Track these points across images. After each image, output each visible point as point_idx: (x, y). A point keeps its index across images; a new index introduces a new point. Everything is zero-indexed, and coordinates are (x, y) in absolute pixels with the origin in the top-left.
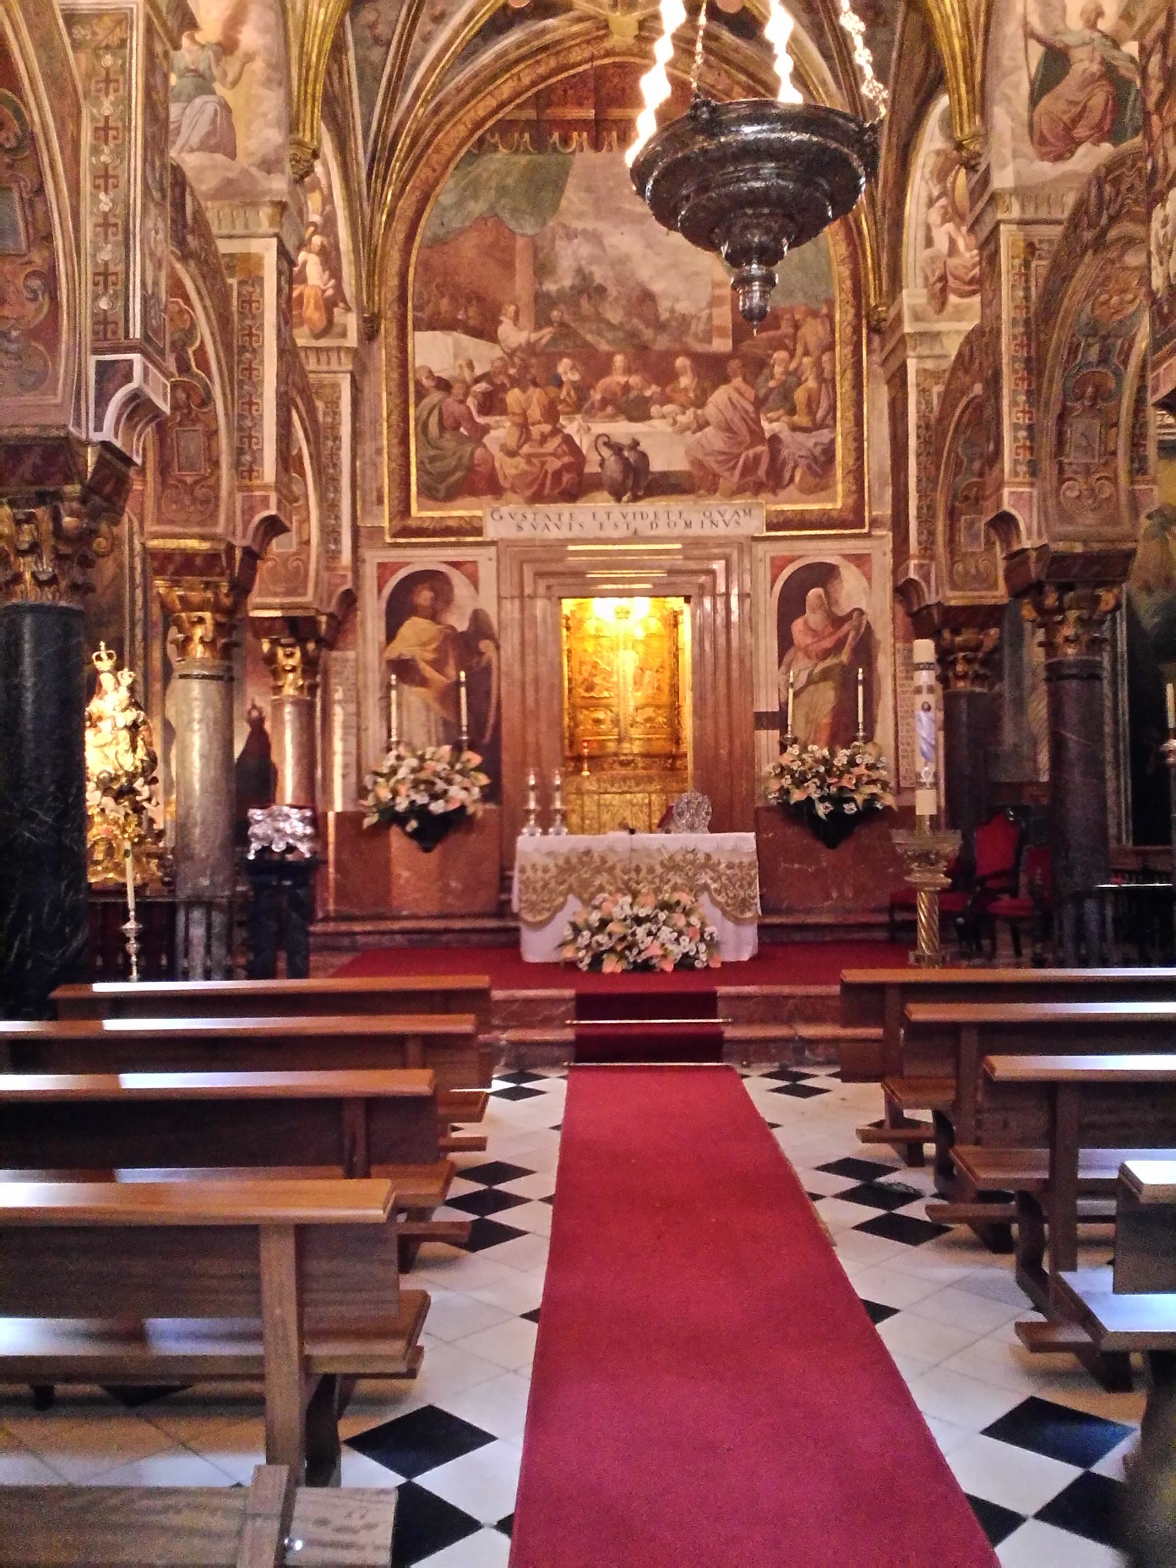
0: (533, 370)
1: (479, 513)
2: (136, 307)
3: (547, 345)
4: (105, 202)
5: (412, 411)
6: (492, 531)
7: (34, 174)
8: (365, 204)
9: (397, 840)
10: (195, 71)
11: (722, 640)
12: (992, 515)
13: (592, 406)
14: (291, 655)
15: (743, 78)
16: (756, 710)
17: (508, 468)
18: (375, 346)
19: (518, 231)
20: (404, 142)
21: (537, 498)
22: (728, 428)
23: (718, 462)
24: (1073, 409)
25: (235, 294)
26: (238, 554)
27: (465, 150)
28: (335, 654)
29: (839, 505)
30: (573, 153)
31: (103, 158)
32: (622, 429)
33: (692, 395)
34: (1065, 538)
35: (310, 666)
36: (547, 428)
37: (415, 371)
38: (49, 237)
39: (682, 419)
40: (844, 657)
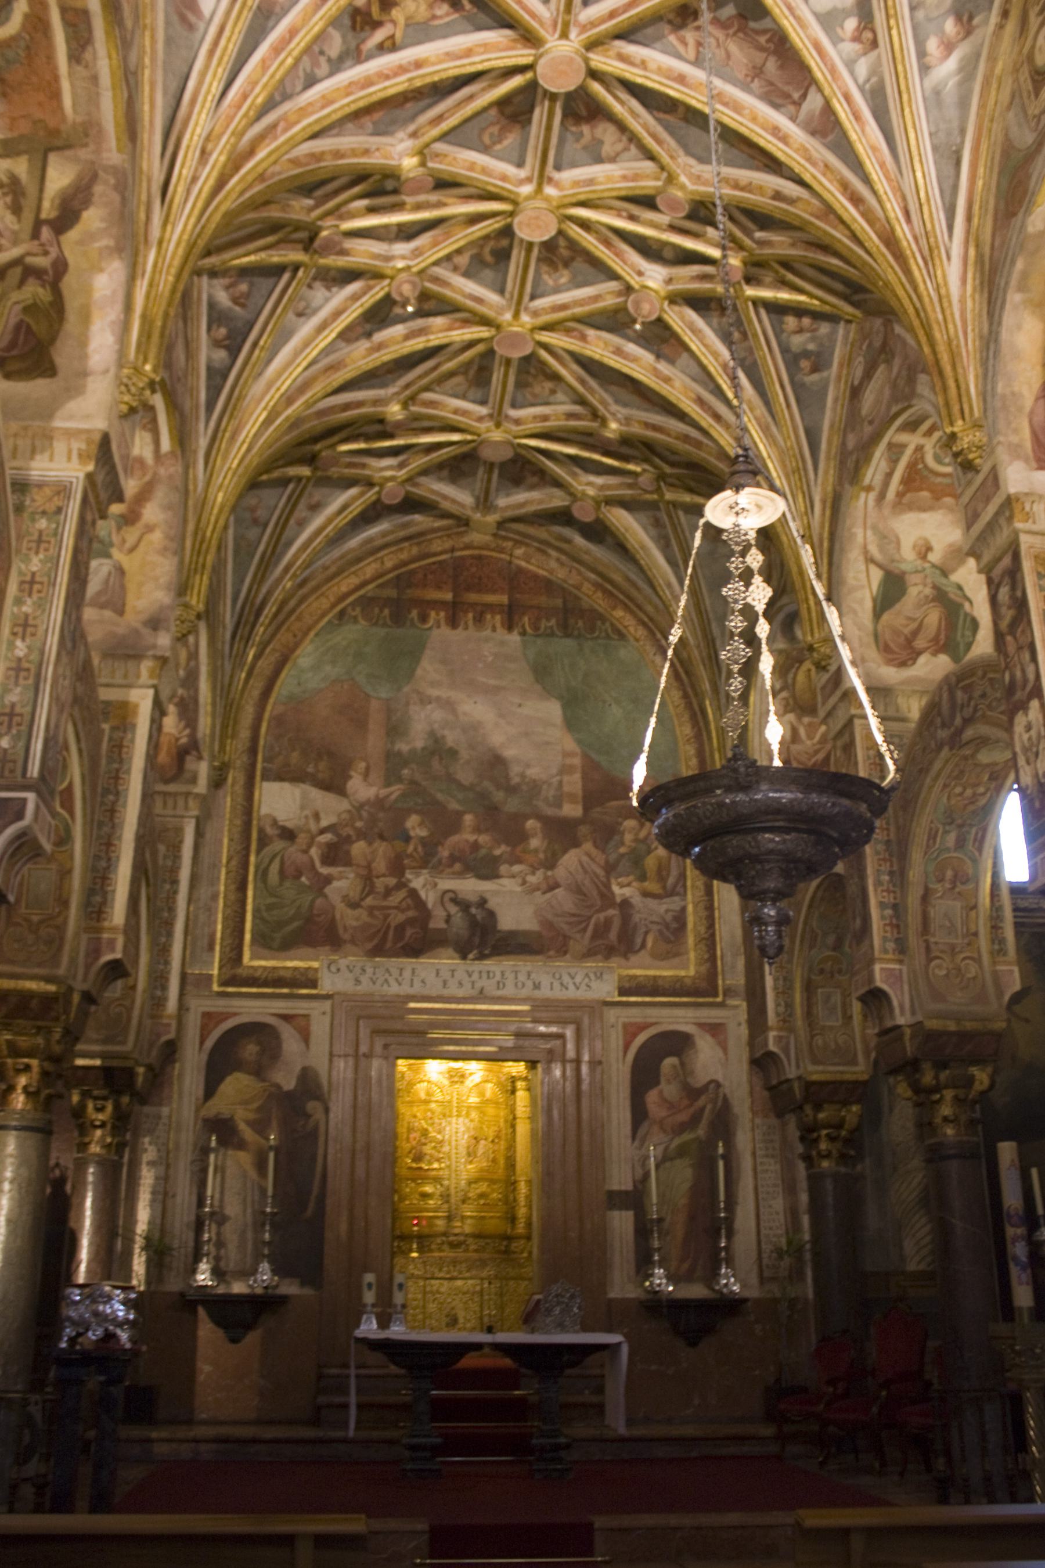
0: (381, 824)
1: (315, 964)
2: (38, 747)
3: (396, 801)
4: (21, 648)
5: (252, 859)
6: (327, 984)
8: (226, 663)
9: (206, 1330)
11: (571, 1109)
12: (862, 991)
13: (440, 862)
14: (100, 1110)
15: (593, 576)
16: (607, 1187)
17: (350, 919)
18: (221, 792)
19: (372, 693)
20: (269, 610)
21: (378, 951)
22: (578, 890)
23: (569, 924)
24: (936, 891)
25: (106, 739)
26: (76, 998)
27: (326, 619)
28: (147, 1109)
29: (692, 972)
30: (430, 629)
31: (25, 609)
32: (470, 887)
33: (541, 856)
34: (939, 1016)
35: (121, 1122)
36: (392, 881)
37: (259, 820)
39: (532, 879)
40: (701, 1132)
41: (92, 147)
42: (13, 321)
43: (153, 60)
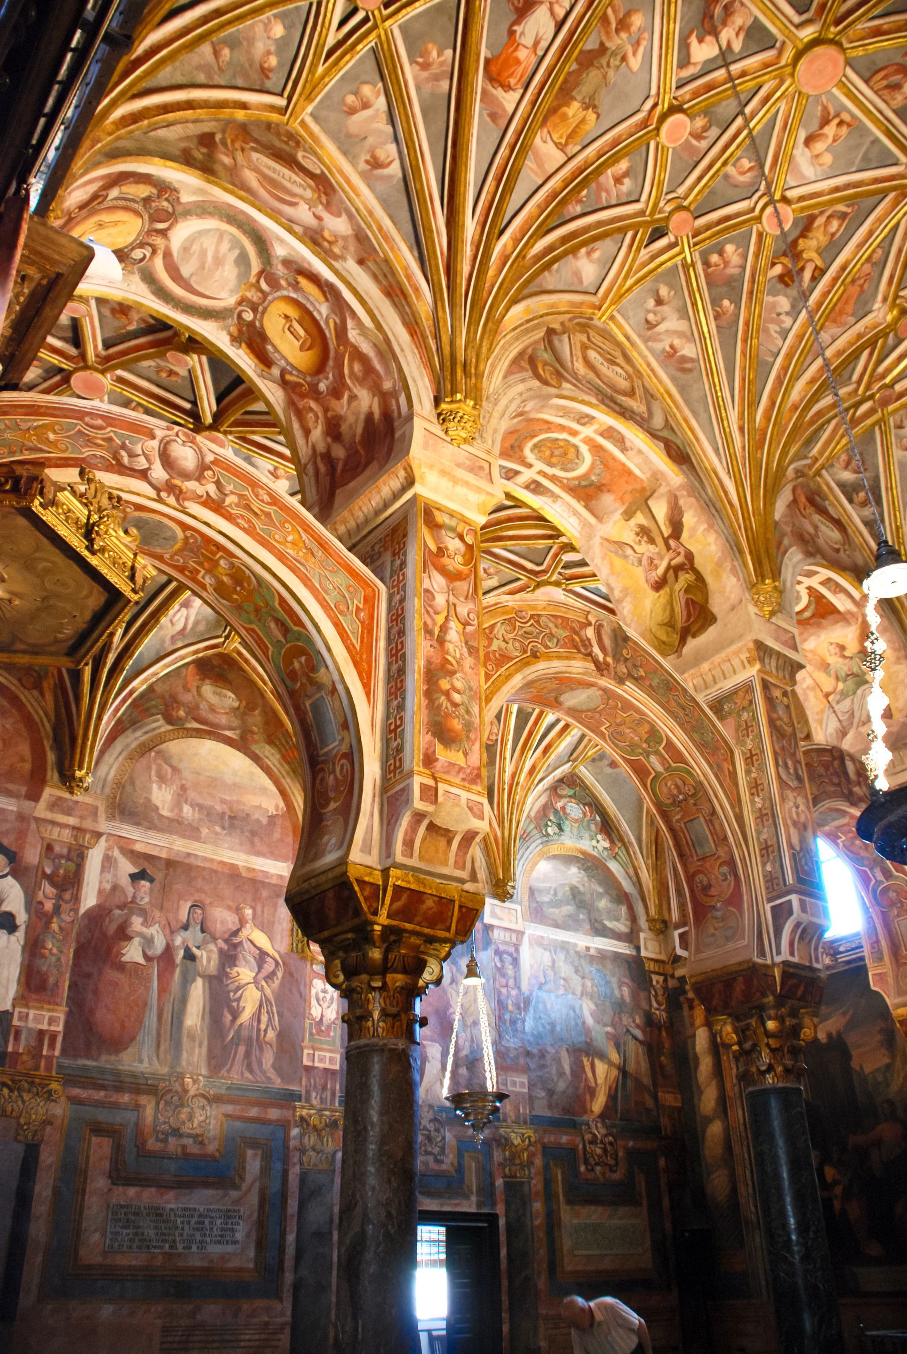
7: (708, 805)
10: (852, 674)
31: (753, 775)
38: (725, 838)
41: (664, 484)
42: (683, 602)
43: (677, 407)
